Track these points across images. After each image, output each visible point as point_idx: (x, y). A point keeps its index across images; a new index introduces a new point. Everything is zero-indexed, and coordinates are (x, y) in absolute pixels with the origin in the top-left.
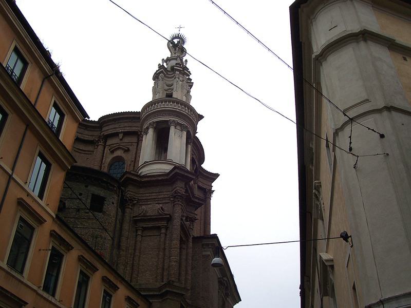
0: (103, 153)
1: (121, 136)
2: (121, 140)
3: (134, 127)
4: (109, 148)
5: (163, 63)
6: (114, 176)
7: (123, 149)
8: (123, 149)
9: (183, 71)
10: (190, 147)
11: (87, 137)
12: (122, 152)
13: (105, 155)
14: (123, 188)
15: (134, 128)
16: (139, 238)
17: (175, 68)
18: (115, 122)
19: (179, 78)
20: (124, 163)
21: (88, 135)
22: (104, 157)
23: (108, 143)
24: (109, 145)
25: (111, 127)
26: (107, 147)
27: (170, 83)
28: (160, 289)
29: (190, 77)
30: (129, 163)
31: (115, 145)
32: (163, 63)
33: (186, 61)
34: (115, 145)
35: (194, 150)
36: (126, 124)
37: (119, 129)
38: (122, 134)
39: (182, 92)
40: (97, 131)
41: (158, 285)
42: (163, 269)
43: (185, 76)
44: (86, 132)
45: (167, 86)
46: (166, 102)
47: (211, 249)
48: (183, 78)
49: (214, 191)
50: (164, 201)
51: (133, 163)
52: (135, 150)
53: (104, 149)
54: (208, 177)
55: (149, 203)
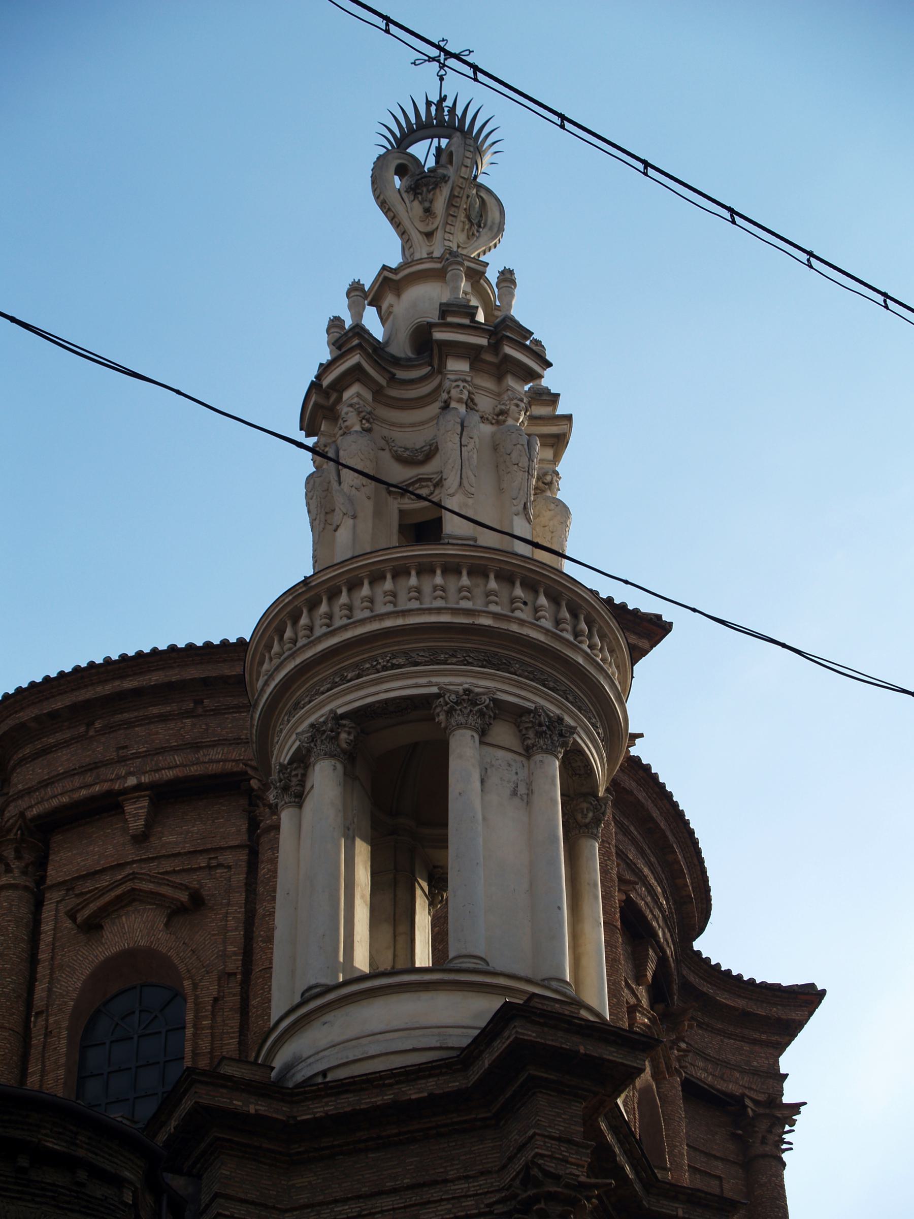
2: (141, 839)
3: (214, 745)
4: (72, 902)
5: (357, 313)
6: (117, 1115)
7: (156, 899)
8: (156, 899)
9: (495, 347)
10: (593, 850)
13: (42, 956)
14: (178, 1183)
15: (216, 754)
17: (438, 335)
18: (90, 724)
19: (470, 404)
20: (177, 995)
22: (42, 970)
23: (54, 874)
24: (68, 885)
25: (64, 760)
26: (53, 897)
27: (416, 439)
29: (544, 382)
30: (210, 989)
31: (105, 881)
32: (357, 313)
33: (507, 278)
34: (105, 881)
35: (632, 854)
36: (162, 733)
38: (145, 803)
39: (501, 490)
43: (511, 382)
45: (399, 459)
46: (400, 572)
48: (499, 395)
49: (796, 1108)
51: (234, 987)
52: (239, 898)
53: (39, 904)
54: (745, 1017)
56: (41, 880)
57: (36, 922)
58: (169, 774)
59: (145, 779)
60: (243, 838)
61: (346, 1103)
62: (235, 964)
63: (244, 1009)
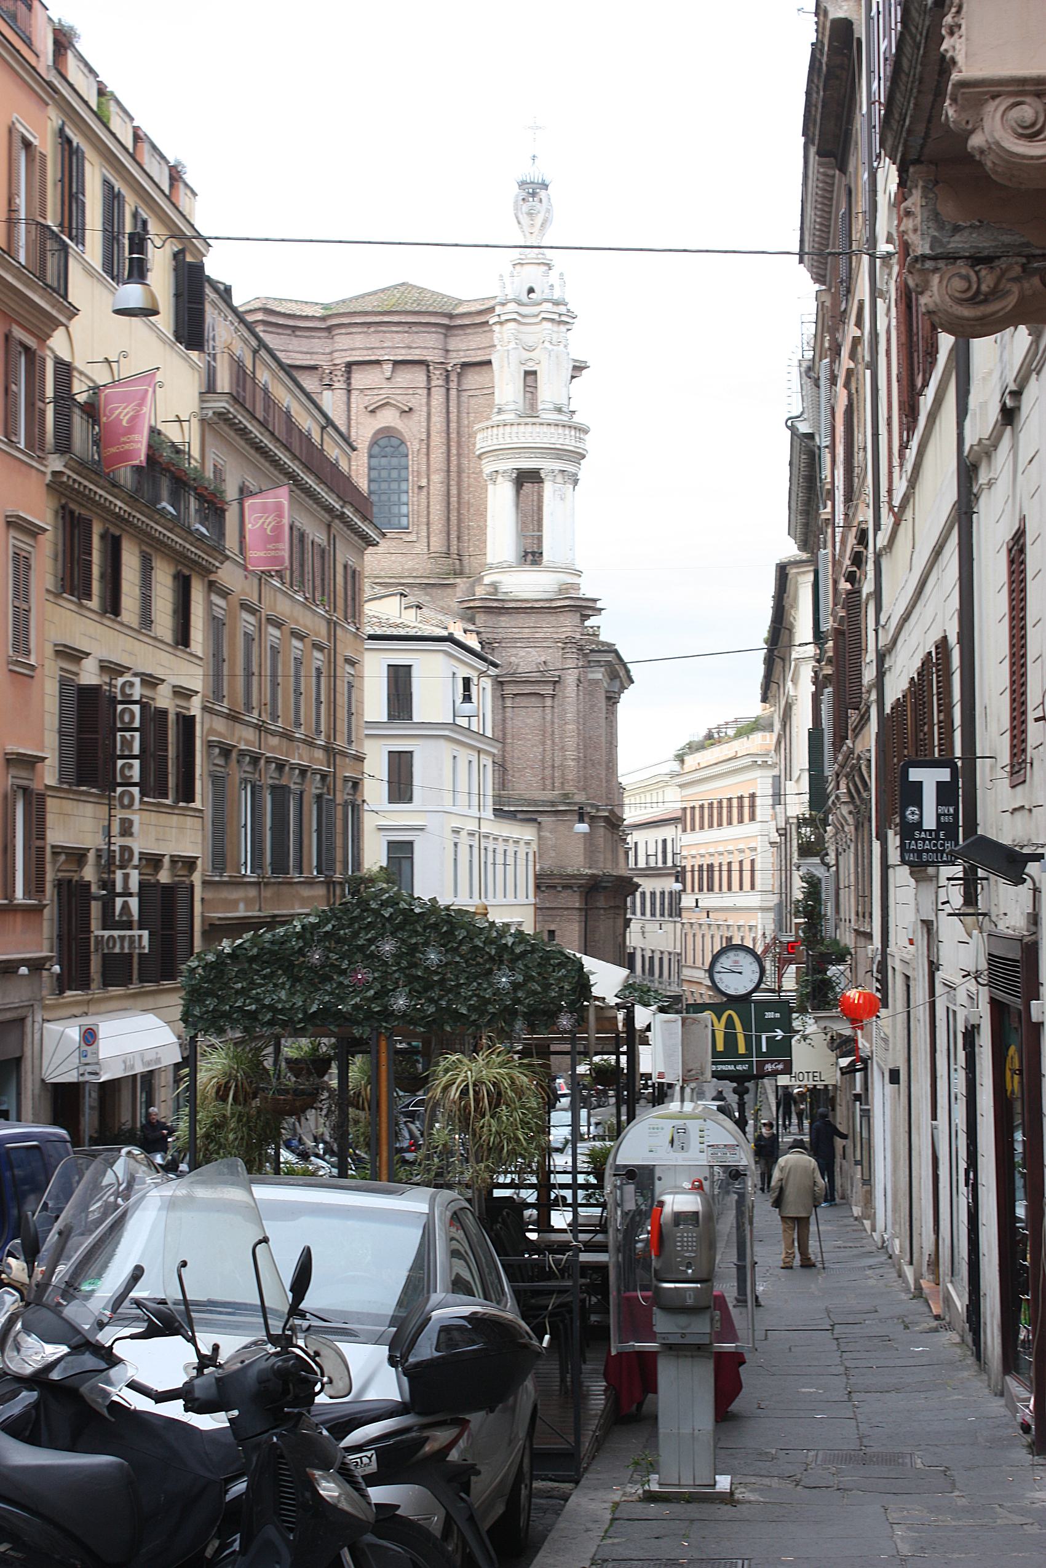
0: (349, 411)
1: (388, 367)
11: (299, 356)
12: (398, 414)
15: (418, 351)
16: (509, 713)
21: (301, 353)
22: (353, 422)
24: (362, 390)
26: (354, 393)
28: (553, 803)
30: (416, 447)
37: (383, 352)
40: (319, 338)
41: (549, 795)
42: (553, 767)
44: (295, 341)
47: (603, 669)
50: (545, 644)
52: (425, 409)
55: (519, 645)
56: (349, 384)
57: (349, 399)
58: (400, 358)
59: (392, 358)
60: (424, 384)
61: (518, 605)
62: (424, 437)
63: (428, 454)
